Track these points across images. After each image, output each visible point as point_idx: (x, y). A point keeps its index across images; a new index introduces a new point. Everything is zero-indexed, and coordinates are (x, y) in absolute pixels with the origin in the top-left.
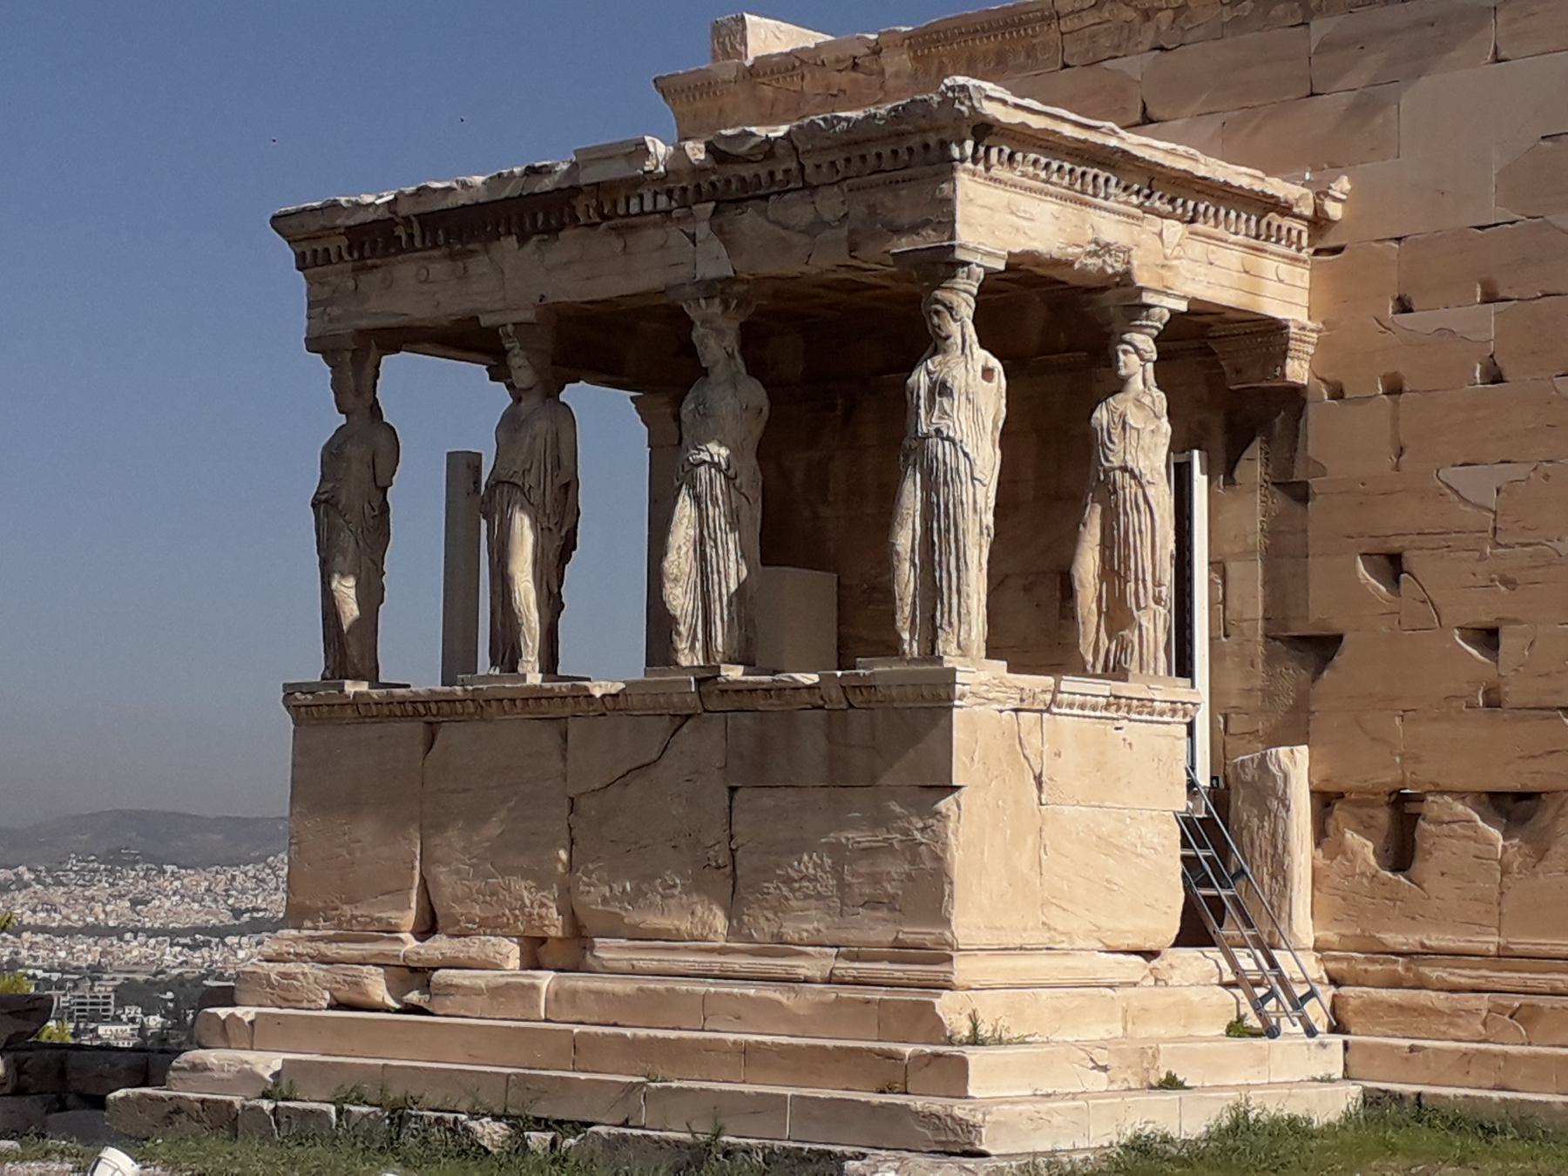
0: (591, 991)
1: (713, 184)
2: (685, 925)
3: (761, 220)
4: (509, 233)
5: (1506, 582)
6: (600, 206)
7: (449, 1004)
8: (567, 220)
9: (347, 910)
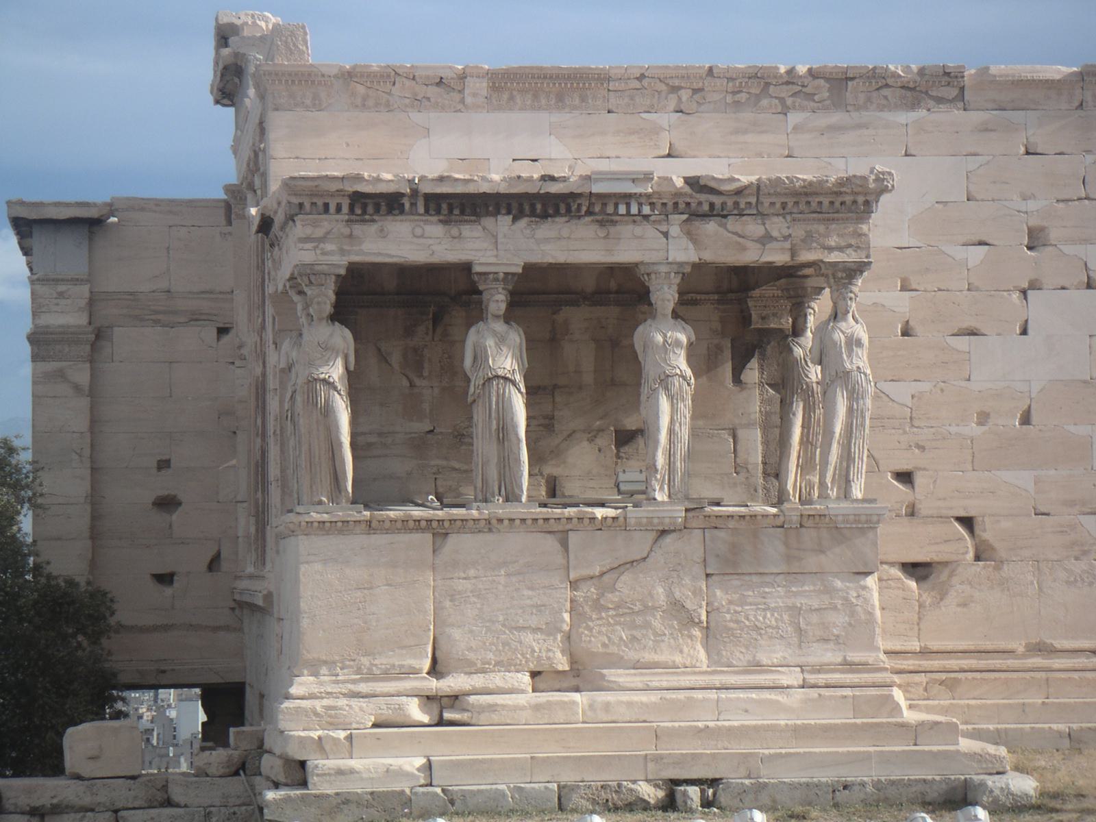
0: (622, 702)
1: (688, 204)
2: (678, 659)
3: (721, 230)
4: (509, 213)
5: (919, 447)
6: (591, 205)
7: (483, 718)
8: (563, 211)
9: (365, 661)
